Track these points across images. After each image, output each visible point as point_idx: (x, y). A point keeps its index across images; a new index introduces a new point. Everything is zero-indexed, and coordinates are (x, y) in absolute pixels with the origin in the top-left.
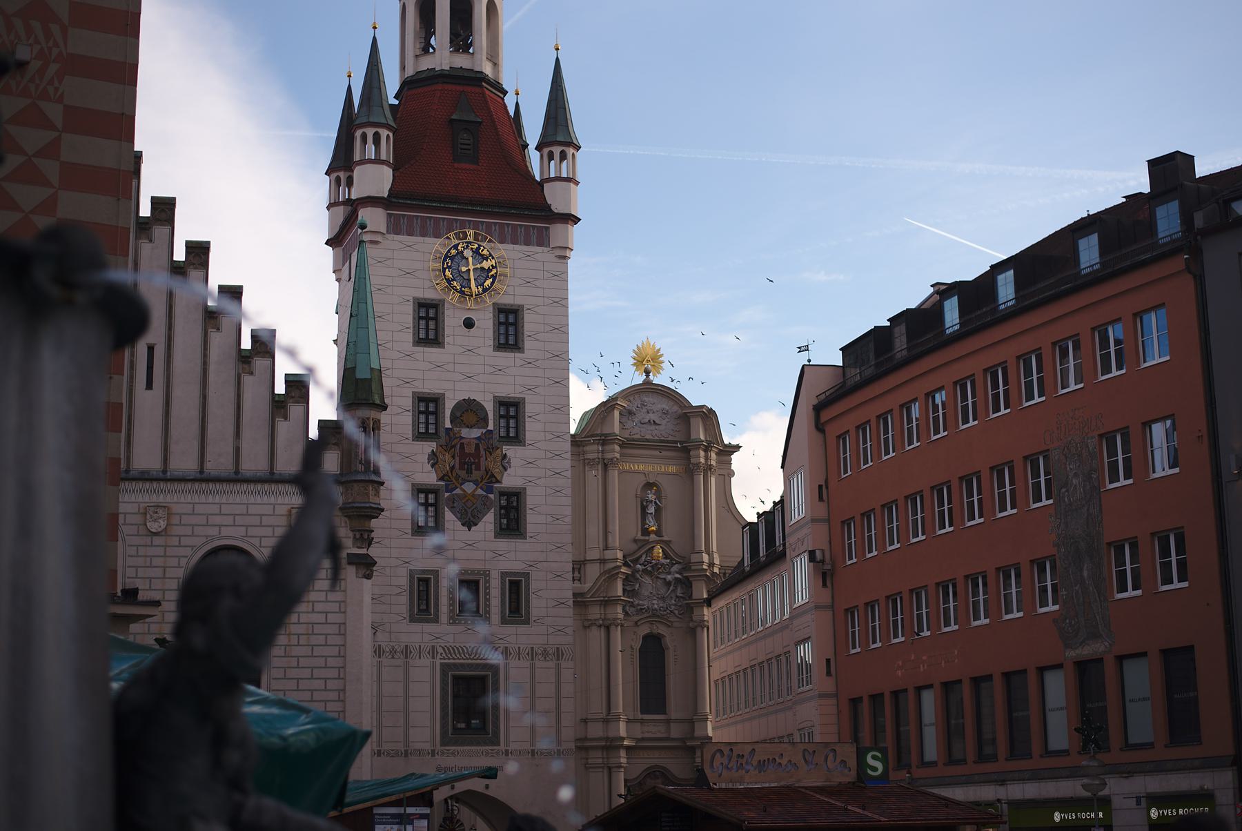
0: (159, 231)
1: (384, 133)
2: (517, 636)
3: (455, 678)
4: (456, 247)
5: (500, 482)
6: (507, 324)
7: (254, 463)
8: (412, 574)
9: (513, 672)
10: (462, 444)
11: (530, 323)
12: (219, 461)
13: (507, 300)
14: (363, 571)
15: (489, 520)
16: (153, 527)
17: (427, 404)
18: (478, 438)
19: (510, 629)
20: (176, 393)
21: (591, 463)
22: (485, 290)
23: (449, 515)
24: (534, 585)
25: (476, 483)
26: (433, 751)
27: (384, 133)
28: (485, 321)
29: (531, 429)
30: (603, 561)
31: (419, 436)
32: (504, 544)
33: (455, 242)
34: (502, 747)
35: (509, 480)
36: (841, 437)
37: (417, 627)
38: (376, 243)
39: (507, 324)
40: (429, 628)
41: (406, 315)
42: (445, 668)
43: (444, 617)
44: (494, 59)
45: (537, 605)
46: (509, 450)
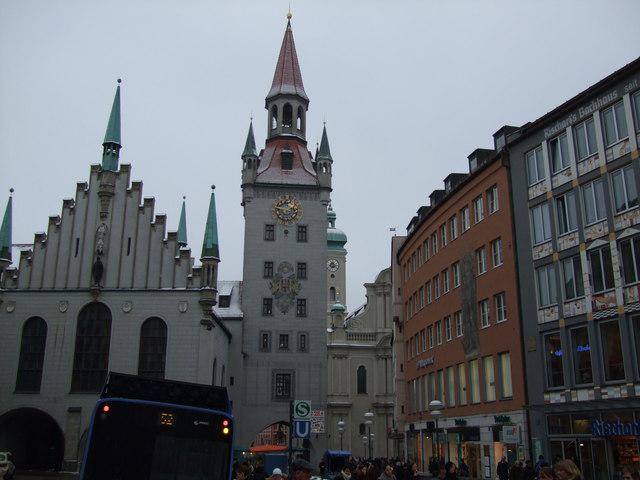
0: (135, 194)
6: (302, 231)
13: (302, 223)
15: (293, 310)
16: (126, 310)
20: (138, 253)
21: (379, 294)
23: (276, 308)
29: (310, 273)
30: (384, 333)
31: (265, 277)
35: (301, 295)
36: (405, 266)
39: (302, 231)
41: (262, 229)
42: (273, 371)
43: (273, 351)
44: (303, 130)
46: (302, 282)
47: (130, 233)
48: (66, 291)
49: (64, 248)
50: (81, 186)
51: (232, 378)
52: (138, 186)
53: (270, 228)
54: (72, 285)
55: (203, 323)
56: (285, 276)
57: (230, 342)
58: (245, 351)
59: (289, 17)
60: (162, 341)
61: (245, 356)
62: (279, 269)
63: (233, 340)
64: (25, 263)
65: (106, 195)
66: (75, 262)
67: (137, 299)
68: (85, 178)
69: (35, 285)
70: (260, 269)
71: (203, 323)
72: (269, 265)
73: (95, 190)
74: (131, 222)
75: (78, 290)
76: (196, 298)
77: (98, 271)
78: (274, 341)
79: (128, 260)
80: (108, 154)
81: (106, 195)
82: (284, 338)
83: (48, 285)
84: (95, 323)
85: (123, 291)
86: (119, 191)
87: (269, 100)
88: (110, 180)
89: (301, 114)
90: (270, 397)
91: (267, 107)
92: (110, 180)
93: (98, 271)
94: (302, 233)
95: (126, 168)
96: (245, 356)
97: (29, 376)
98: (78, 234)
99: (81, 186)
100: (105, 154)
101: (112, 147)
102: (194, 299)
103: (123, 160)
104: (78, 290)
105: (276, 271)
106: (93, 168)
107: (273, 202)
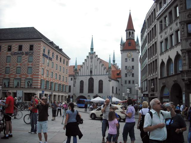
2: (133, 85)
7: (103, 74)
11: (135, 59)
12: (100, 74)
15: (131, 75)
17: (126, 67)
31: (126, 69)
32: (133, 78)
34: (132, 94)
35: (133, 73)
43: (127, 83)
46: (133, 70)
48: (86, 76)
49: (85, 68)
50: (87, 56)
51: (119, 89)
52: (97, 56)
53: (126, 59)
54: (87, 75)
55: (109, 80)
56: (129, 69)
59: (130, 11)
60: (102, 84)
61: (122, 85)
63: (119, 82)
64: (79, 71)
65: (92, 58)
66: (87, 70)
67: (97, 76)
68: (88, 55)
70: (124, 68)
71: (109, 80)
72: (126, 67)
73: (90, 57)
74: (96, 63)
75: (88, 75)
76: (108, 76)
77: (91, 72)
78: (128, 82)
79: (96, 70)
81: (92, 58)
82: (129, 82)
83: (83, 75)
84: (91, 81)
86: (94, 57)
87: (126, 31)
88: (92, 55)
89: (133, 33)
92: (92, 55)
93: (91, 72)
94: (133, 60)
95: (95, 53)
96: (122, 85)
97: (82, 90)
99: (87, 56)
100: (91, 50)
101: (92, 49)
102: (107, 76)
103: (94, 51)
104: (88, 75)
105: (128, 68)
106: (89, 53)
107: (127, 53)
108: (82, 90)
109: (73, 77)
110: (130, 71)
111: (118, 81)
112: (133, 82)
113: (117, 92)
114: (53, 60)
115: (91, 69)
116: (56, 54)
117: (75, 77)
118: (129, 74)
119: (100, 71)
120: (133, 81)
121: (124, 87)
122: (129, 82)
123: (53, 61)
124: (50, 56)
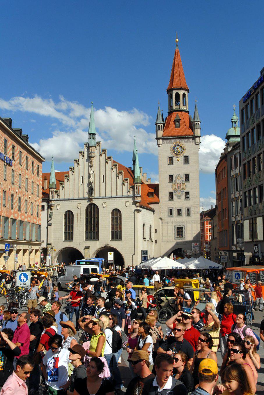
1: (160, 125)
3: (177, 227)
4: (175, 145)
5: (184, 190)
7: (119, 195)
8: (168, 208)
9: (188, 226)
10: (177, 184)
13: (186, 155)
14: (137, 212)
15: (183, 197)
16: (104, 206)
18: (181, 182)
19: (188, 218)
22: (181, 153)
24: (192, 209)
25: (180, 190)
26: (173, 241)
27: (160, 125)
28: (182, 159)
29: (190, 178)
31: (170, 182)
32: (187, 202)
33: (175, 144)
35: (187, 190)
37: (169, 218)
38: (160, 146)
40: (172, 218)
41: (167, 160)
43: (174, 216)
45: (192, 213)
46: (187, 183)
47: (103, 173)
51: (156, 230)
53: (171, 159)
54: (81, 197)
56: (179, 181)
57: (154, 214)
58: (161, 217)
61: (161, 219)
62: (176, 178)
63: (155, 213)
66: (81, 187)
69: (67, 197)
72: (171, 177)
74: (103, 168)
77: (91, 190)
78: (175, 212)
79: (103, 185)
80: (90, 138)
83: (71, 197)
84: (92, 212)
85: (103, 198)
90: (174, 237)
91: (168, 94)
93: (91, 190)
98: (81, 174)
102: (131, 200)
105: (174, 179)
108: (69, 235)
109: (45, 204)
110: (179, 187)
111: (153, 211)
112: (188, 214)
113: (152, 237)
114: (14, 166)
115: (90, 183)
116: (19, 150)
117: (50, 203)
118: (179, 193)
119: (114, 187)
120: (188, 210)
121: (167, 223)
122: (179, 211)
123: (13, 167)
124: (8, 156)
